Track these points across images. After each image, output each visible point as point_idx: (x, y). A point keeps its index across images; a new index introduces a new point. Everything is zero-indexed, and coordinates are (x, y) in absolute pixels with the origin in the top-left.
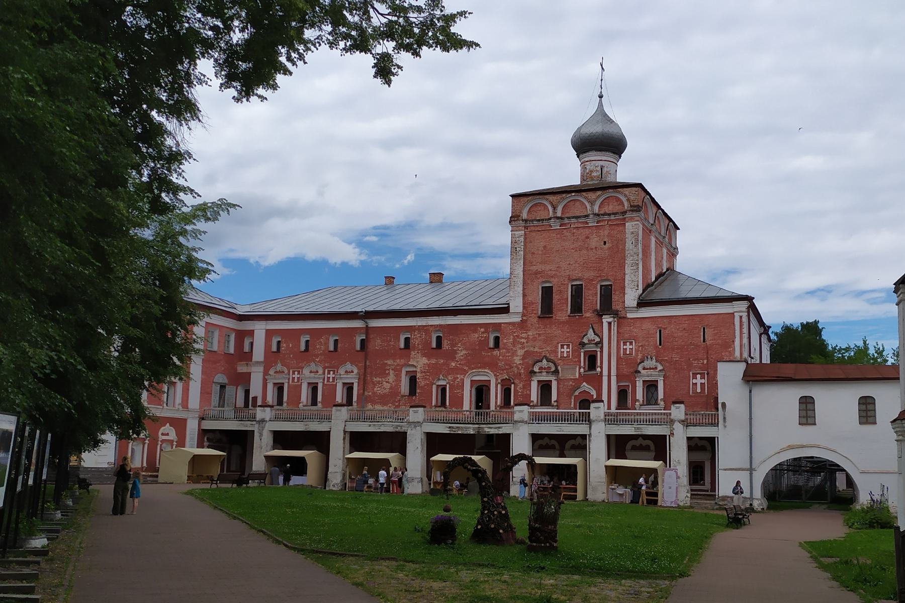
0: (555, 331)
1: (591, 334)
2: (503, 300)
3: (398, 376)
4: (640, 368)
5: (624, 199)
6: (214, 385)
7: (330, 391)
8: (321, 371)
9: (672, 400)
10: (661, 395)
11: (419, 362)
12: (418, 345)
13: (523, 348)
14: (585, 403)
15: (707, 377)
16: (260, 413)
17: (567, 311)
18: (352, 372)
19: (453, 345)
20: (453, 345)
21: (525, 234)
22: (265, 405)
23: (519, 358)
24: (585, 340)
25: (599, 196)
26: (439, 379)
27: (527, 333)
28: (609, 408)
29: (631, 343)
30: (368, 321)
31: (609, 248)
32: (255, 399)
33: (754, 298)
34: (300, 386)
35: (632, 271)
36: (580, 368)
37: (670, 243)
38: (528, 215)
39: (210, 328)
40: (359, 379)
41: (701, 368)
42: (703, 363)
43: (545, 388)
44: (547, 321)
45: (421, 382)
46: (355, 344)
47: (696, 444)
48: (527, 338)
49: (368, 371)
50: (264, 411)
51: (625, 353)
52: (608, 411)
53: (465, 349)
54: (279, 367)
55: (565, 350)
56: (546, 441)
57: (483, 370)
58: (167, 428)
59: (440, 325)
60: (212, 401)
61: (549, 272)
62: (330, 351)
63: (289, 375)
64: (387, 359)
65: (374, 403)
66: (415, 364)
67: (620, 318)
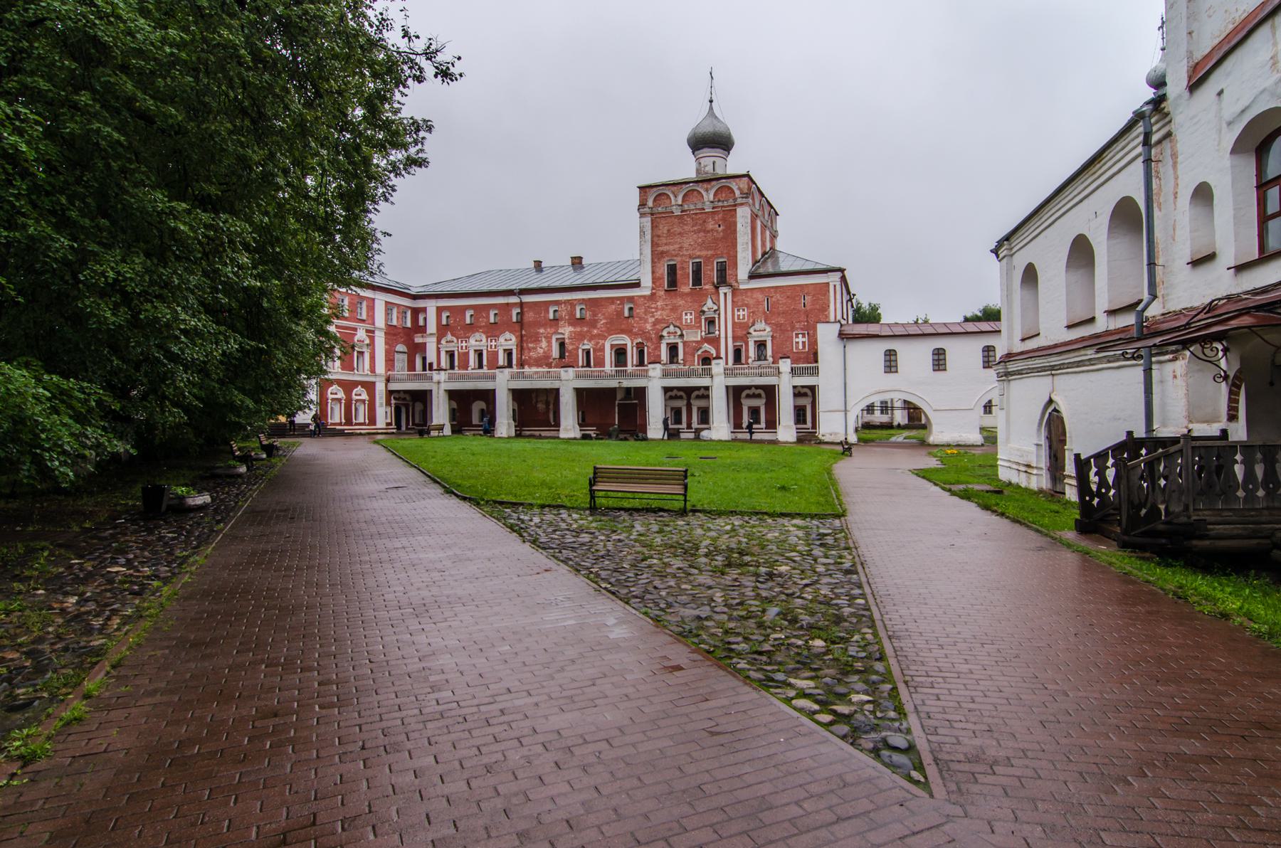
2: (635, 277)
3: (549, 343)
4: (751, 330)
5: (735, 188)
7: (493, 356)
8: (484, 340)
9: (780, 355)
10: (769, 352)
11: (566, 331)
13: (653, 316)
14: (706, 360)
16: (436, 376)
19: (595, 315)
20: (595, 315)
21: (652, 220)
22: (440, 369)
24: (705, 308)
25: (713, 187)
28: (727, 363)
29: (744, 310)
30: (521, 297)
31: (723, 231)
32: (431, 365)
34: (468, 353)
37: (772, 226)
39: (389, 306)
41: (802, 329)
43: (673, 349)
44: (672, 293)
45: (569, 347)
46: (511, 317)
47: (799, 392)
49: (525, 338)
50: (439, 374)
51: (739, 318)
53: (604, 318)
54: (449, 337)
55: (689, 317)
56: (675, 392)
58: (359, 389)
65: (530, 366)
66: (563, 332)
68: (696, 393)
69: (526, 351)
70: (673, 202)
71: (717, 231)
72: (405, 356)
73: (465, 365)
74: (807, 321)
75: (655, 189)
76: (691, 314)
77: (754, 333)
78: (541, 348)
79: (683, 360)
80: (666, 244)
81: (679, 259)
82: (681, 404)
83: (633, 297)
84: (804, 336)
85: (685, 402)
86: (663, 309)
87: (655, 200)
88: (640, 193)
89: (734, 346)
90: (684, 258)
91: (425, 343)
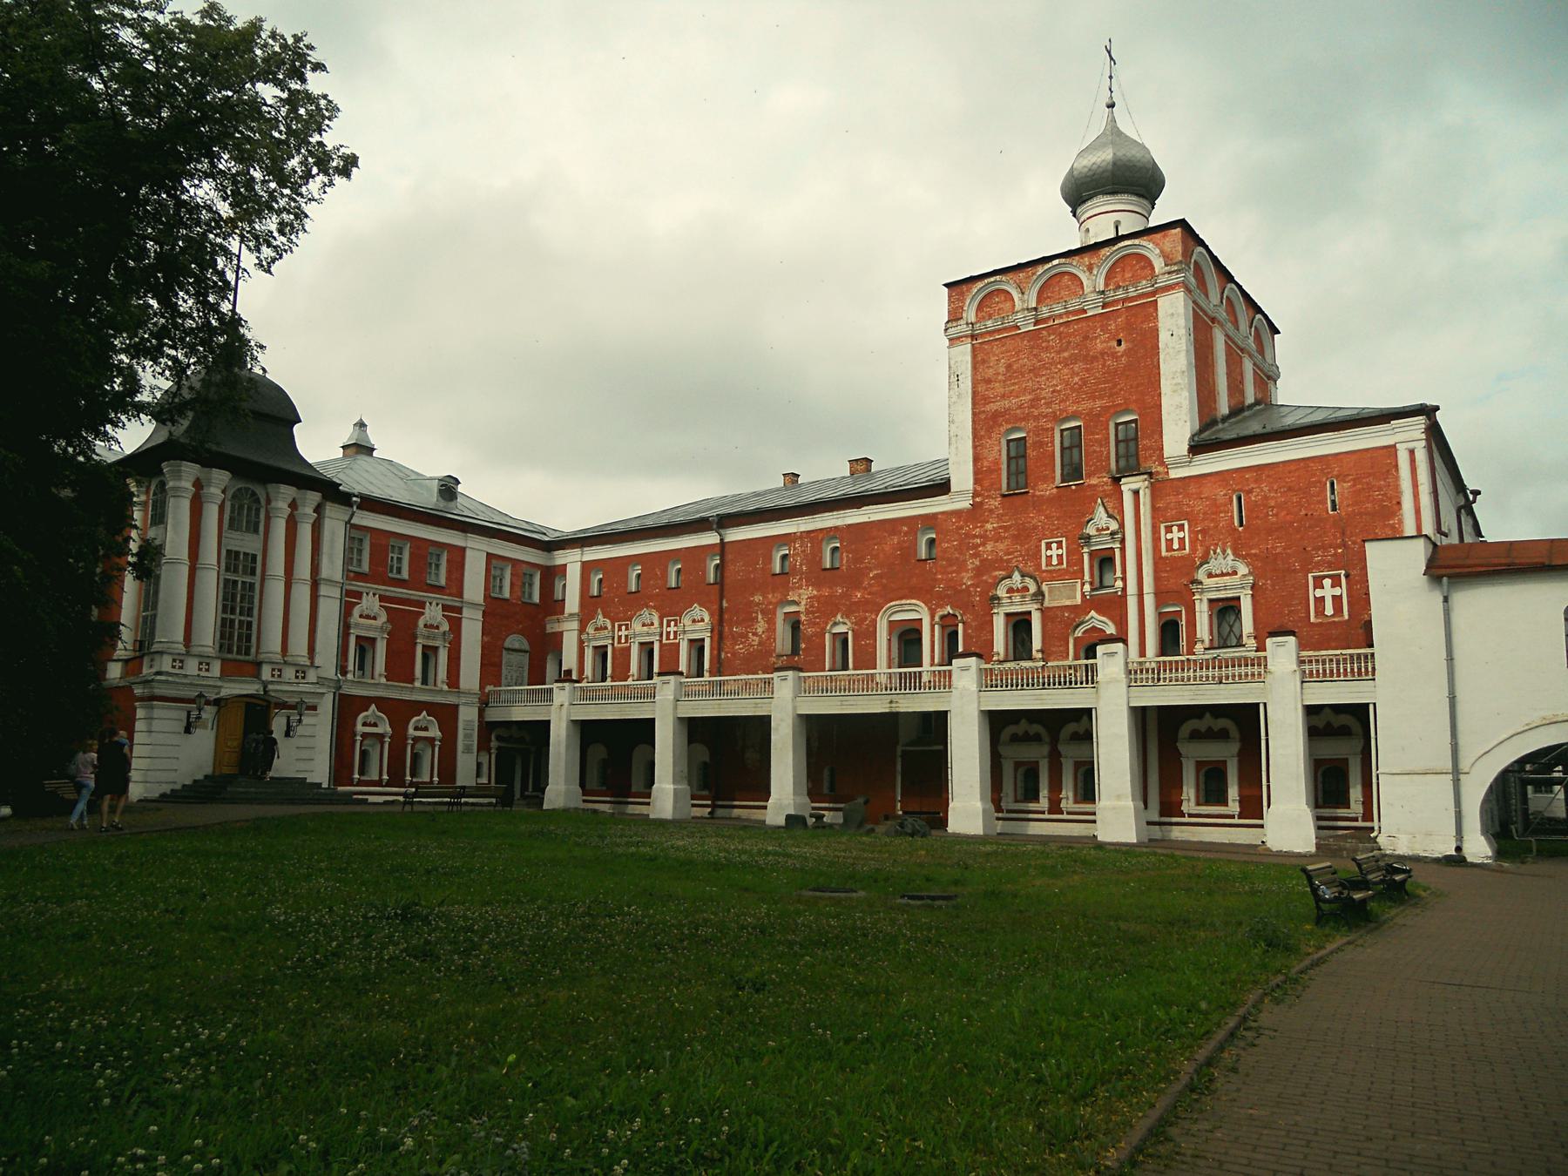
0: (1035, 519)
1: (1101, 516)
3: (771, 623)
4: (1201, 575)
6: (504, 652)
7: (671, 652)
11: (802, 597)
12: (801, 565)
13: (975, 556)
15: (1347, 583)
17: (1054, 478)
18: (703, 620)
23: (970, 574)
24: (1090, 530)
26: (835, 624)
27: (981, 527)
28: (1142, 653)
29: (1181, 528)
30: (722, 531)
32: (569, 672)
33: (1437, 408)
35: (1175, 388)
36: (1083, 584)
38: (977, 315)
40: (712, 632)
42: (1335, 554)
43: (1020, 625)
44: (1017, 501)
45: (807, 630)
46: (704, 572)
47: (1329, 724)
48: (980, 536)
49: (726, 617)
51: (1170, 548)
52: (1142, 659)
54: (601, 619)
55: (1054, 552)
57: (908, 602)
59: (836, 528)
60: (503, 678)
61: (1018, 411)
62: (669, 589)
63: (613, 631)
64: (753, 596)
66: (796, 599)
67: (1157, 480)
68: (1071, 727)
69: (728, 643)
70: (1018, 305)
71: (1114, 355)
72: (525, 659)
73: (622, 672)
74: (1344, 545)
75: (980, 285)
76: (1060, 545)
77: (1208, 582)
78: (755, 634)
79: (1042, 651)
80: (1003, 396)
81: (1031, 425)
82: (1038, 753)
83: (934, 516)
84: (1336, 582)
85: (1045, 750)
86: (998, 539)
87: (979, 308)
88: (950, 296)
89: (1161, 615)
90: (1042, 422)
91: (562, 633)
